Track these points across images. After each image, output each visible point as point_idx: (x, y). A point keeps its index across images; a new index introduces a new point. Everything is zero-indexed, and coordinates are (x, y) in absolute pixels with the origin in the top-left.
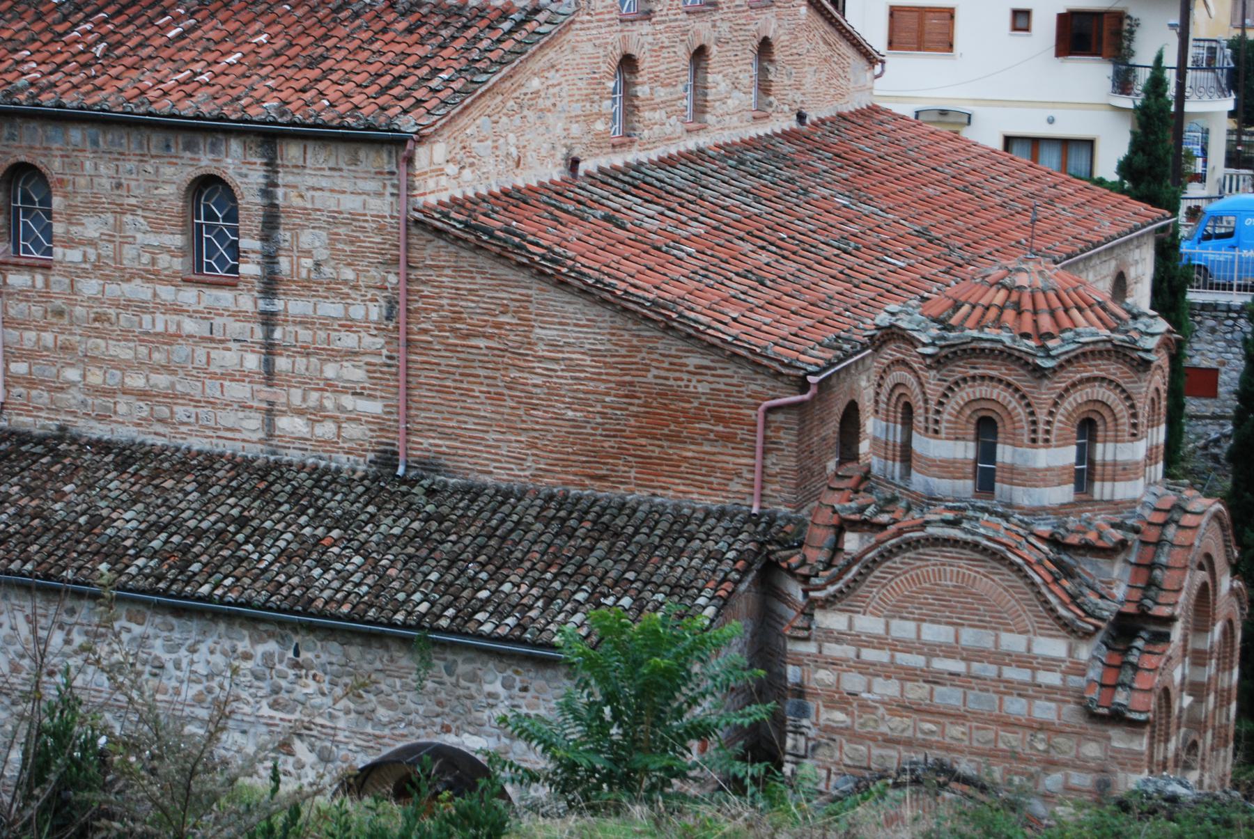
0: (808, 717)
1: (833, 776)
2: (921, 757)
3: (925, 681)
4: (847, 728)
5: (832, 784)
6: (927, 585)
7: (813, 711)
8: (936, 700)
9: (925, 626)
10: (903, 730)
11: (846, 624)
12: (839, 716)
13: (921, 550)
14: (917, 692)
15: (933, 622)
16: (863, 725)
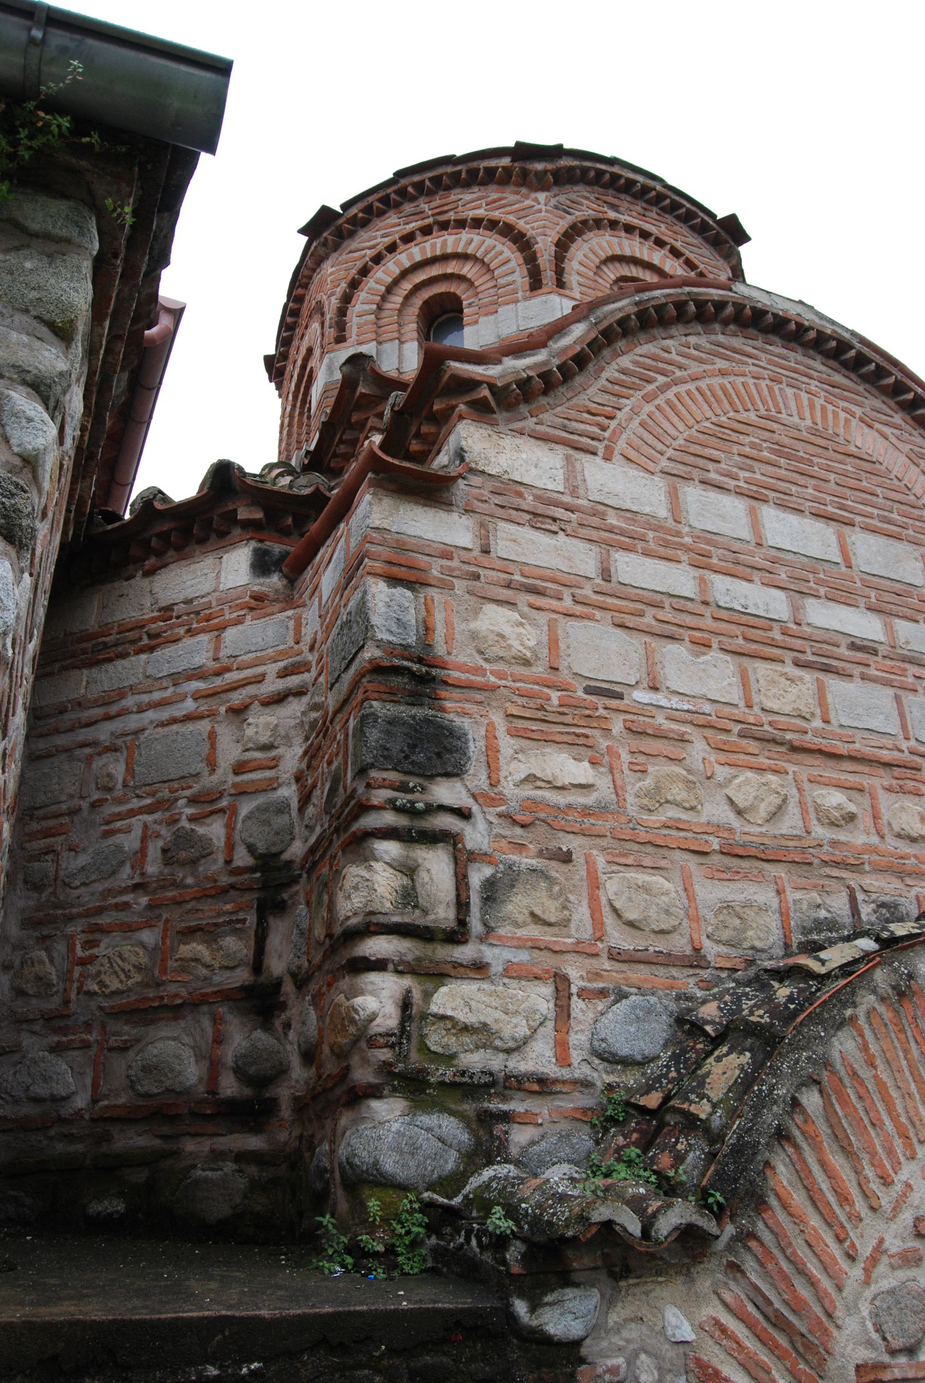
0: (455, 772)
1: (577, 1005)
2: (839, 905)
3: (797, 664)
4: (601, 810)
5: (578, 1039)
6: (752, 416)
7: (475, 748)
8: (840, 717)
9: (769, 514)
10: (776, 814)
11: (560, 474)
12: (568, 767)
13: (721, 338)
14: (785, 692)
15: (781, 505)
16: (656, 798)
